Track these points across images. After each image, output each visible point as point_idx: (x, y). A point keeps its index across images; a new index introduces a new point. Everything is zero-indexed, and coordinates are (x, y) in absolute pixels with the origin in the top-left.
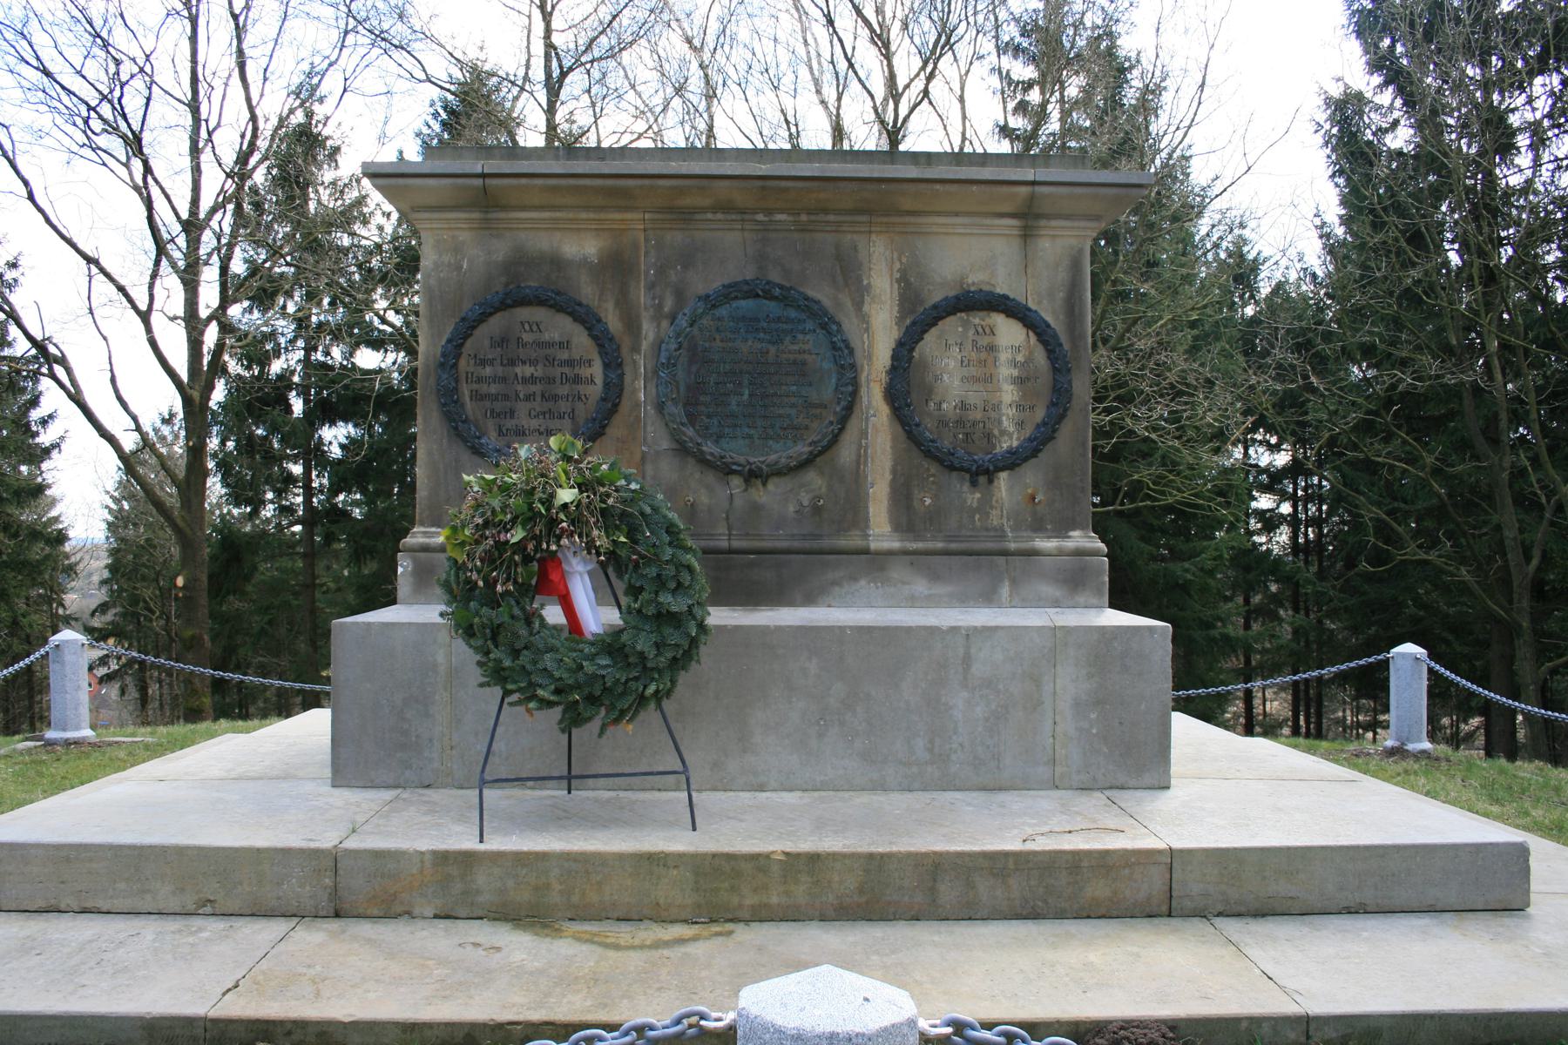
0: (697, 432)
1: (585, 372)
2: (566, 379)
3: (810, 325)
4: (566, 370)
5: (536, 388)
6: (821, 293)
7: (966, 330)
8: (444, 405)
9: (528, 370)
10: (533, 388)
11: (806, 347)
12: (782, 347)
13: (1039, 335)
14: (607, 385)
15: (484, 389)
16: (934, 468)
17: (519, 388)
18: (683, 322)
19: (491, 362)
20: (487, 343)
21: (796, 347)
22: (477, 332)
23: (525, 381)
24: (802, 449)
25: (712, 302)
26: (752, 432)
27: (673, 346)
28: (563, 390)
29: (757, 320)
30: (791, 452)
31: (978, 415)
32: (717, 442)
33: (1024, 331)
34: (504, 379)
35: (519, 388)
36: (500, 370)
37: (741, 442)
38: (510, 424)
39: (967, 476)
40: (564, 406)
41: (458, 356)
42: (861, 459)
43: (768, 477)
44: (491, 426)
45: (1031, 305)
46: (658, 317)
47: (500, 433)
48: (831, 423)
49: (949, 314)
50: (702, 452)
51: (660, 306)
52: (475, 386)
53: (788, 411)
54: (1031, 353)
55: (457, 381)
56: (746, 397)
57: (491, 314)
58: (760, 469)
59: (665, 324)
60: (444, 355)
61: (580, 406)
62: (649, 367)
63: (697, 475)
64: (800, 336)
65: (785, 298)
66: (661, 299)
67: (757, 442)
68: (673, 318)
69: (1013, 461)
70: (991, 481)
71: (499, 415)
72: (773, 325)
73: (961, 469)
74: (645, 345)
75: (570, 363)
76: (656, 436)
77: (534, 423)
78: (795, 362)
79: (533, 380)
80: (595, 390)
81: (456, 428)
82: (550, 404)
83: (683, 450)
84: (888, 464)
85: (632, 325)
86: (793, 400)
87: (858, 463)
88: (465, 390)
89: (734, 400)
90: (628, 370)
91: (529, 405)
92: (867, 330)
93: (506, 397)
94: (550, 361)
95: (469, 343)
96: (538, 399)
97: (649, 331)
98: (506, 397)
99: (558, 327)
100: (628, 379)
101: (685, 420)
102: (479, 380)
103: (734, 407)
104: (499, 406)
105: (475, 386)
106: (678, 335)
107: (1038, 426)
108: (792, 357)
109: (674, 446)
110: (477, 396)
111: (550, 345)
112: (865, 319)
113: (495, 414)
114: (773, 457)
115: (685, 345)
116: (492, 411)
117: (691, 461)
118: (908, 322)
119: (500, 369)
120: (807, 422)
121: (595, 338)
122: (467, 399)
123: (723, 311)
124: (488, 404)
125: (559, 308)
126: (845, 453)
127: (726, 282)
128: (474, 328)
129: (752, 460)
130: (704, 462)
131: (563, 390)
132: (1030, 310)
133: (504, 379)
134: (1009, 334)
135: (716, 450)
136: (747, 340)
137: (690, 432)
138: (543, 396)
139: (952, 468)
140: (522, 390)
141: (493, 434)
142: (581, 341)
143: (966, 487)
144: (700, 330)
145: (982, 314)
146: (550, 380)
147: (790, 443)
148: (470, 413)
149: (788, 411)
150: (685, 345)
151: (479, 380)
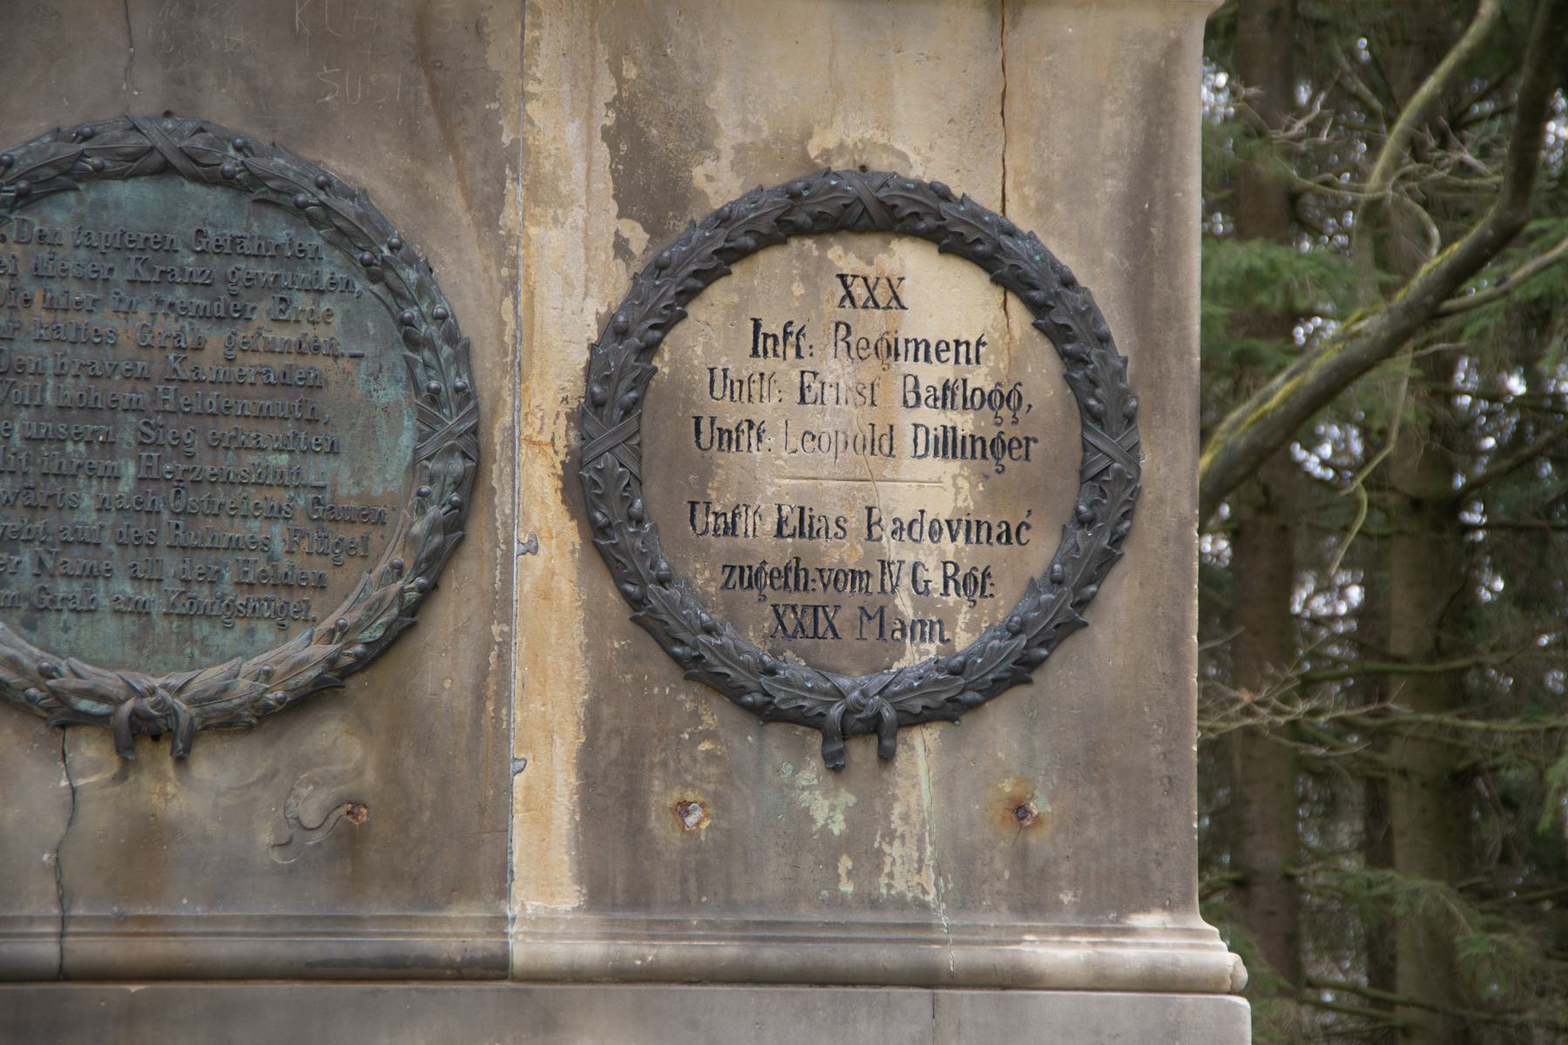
3: (331, 266)
11: (322, 333)
12: (244, 332)
24: (303, 651)
32: (30, 625)
43: (193, 736)
48: (399, 570)
56: (125, 487)
58: (172, 713)
64: (302, 301)
86: (280, 496)
103: (87, 515)
108: (277, 364)
114: (210, 676)
120: (320, 565)
127: (68, 122)
129: (144, 681)
147: (265, 631)
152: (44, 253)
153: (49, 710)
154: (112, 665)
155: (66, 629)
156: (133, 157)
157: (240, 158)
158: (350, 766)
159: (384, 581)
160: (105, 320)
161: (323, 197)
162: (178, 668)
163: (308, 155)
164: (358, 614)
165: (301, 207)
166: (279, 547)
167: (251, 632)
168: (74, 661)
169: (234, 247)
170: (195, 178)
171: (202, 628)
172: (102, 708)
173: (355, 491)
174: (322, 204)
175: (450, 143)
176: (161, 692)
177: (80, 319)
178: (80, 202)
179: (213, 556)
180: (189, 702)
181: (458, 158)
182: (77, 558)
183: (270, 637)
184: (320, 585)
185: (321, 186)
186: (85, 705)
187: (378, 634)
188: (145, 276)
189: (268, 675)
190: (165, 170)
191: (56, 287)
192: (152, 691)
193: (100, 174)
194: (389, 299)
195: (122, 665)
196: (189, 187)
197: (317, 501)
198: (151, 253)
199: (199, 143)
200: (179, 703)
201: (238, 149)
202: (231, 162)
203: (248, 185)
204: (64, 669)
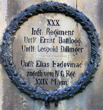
13: (83, 25)
31: (50, 69)
33: (75, 23)
39: (44, 103)
49: (35, 14)
54: (79, 35)
69: (68, 95)
70: (56, 106)
73: (39, 99)
107: (82, 75)
132: (78, 11)
134: (66, 24)
139: (34, 99)
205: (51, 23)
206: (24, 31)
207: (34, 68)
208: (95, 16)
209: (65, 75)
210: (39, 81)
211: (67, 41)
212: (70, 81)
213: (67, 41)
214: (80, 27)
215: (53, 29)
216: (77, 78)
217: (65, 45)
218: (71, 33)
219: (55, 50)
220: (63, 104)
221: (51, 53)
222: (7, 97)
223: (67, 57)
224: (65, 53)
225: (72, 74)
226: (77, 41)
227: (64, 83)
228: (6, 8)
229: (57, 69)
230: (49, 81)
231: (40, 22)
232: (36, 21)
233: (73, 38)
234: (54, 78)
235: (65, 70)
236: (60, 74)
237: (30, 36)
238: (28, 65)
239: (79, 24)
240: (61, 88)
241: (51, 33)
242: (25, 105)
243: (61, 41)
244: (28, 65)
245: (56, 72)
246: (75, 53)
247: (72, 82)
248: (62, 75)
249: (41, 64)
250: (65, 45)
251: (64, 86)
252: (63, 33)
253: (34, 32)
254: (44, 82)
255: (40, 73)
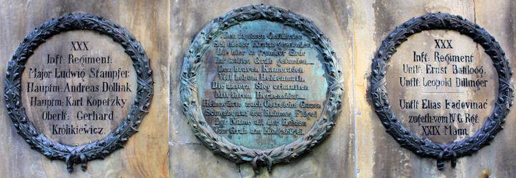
0: (214, 129)
1: (122, 81)
2: (107, 87)
3: (305, 40)
4: (107, 80)
5: (84, 95)
6: (313, 16)
7: (429, 45)
8: (9, 109)
9: (75, 81)
10: (80, 95)
11: (302, 58)
12: (282, 58)
13: (485, 47)
14: (139, 91)
15: (42, 96)
16: (407, 155)
17: (70, 95)
18: (201, 40)
19: (48, 74)
20: (45, 59)
21: (294, 59)
22: (37, 52)
23: (74, 89)
24: (301, 142)
25: (226, 24)
26: (260, 128)
27: (193, 59)
28: (104, 96)
29: (262, 37)
30: (290, 146)
31: (441, 112)
32: (230, 137)
33: (474, 44)
34: (57, 88)
35: (70, 95)
36: (54, 81)
37: (250, 137)
38: (62, 124)
39: (435, 162)
40: (105, 109)
41: (21, 71)
42: (349, 149)
43: (274, 165)
44: (46, 125)
45: (478, 23)
46: (181, 37)
47: (54, 131)
48: (325, 120)
49: (417, 31)
50: (217, 146)
51: (183, 27)
52: (34, 94)
53: (287, 110)
54: (480, 61)
55: (20, 90)
56: (254, 100)
57: (48, 37)
58: (266, 160)
59: (186, 41)
60: (9, 70)
61: (118, 109)
62: (174, 76)
63: (215, 165)
64: (297, 50)
65: (285, 19)
66: (184, 22)
67: (264, 137)
68: (193, 37)
69: (470, 150)
70: (453, 165)
71: (53, 117)
72: (275, 41)
73: (431, 156)
74: (171, 59)
75: (110, 74)
76: (181, 136)
77: (81, 124)
78: (293, 71)
79: (80, 88)
80: (130, 96)
81: (18, 128)
82: (94, 108)
83: (202, 144)
84: (372, 152)
85: (160, 43)
86: (293, 102)
87: (347, 153)
88: (27, 97)
89: (243, 102)
90: (157, 78)
91: (78, 108)
92: (351, 44)
93: (59, 102)
94: (94, 73)
95: (30, 60)
96: (85, 103)
97: (174, 48)
98: (59, 102)
99: (100, 46)
100: (157, 87)
101: (203, 120)
102: (38, 89)
103: (243, 109)
104: (53, 110)
105: (34, 94)
106: (198, 50)
108: (291, 66)
109: (195, 141)
110: (35, 102)
111: (94, 60)
112: (348, 36)
113: (50, 116)
114: (277, 150)
115: (203, 58)
116: (48, 114)
117: (209, 154)
118: (384, 37)
119: (55, 80)
120: (304, 119)
121: (130, 54)
122: (28, 104)
123: (234, 31)
124: (44, 108)
125: (100, 31)
126: (336, 145)
128: (34, 48)
129: (259, 152)
130: (219, 154)
131: (104, 96)
132: (478, 27)
133: (57, 88)
134: (462, 45)
135: (230, 145)
136: (253, 54)
137: (208, 129)
138: (88, 101)
139: (422, 156)
140: (72, 97)
141: (49, 132)
142: (119, 57)
143: (434, 169)
144: (216, 46)
145: (441, 32)
146: (94, 89)
147: (290, 137)
148: (30, 115)
149: (287, 110)
150: (203, 58)
151: (38, 89)
152: (231, 40)
153: (235, 160)
154: (251, 147)
155: (239, 138)
156: (253, 15)
157: (280, 14)
158: (314, 173)
159: (321, 124)
160: (246, 57)
161: (302, 22)
162: (268, 148)
163: (297, 13)
164: (316, 132)
165: (297, 25)
166: (293, 114)
167: (287, 138)
168: (242, 147)
169: (280, 36)
170: (268, 19)
171: (275, 137)
172: (249, 159)
173: (313, 99)
174: (302, 25)
175: (333, 8)
176: (264, 155)
177: (240, 57)
178: (240, 27)
179: (276, 118)
180: (272, 157)
181: (336, 13)
182: (241, 119)
183: (292, 139)
184: (304, 124)
185: (302, 20)
186: (245, 158)
187: (321, 137)
188: (257, 45)
189: (292, 149)
190: (262, 18)
191: (234, 49)
192: (262, 155)
193: (245, 20)
194: (320, 49)
195: (254, 148)
196: (267, 22)
197: (303, 102)
198: (258, 41)
199: (270, 10)
200: (269, 158)
201: (280, 11)
202: (278, 15)
203: (284, 20)
204: (239, 149)
205: (440, 44)
206: (402, 56)
207: (420, 111)
208: (502, 33)
209: (464, 119)
210: (427, 130)
211: (464, 70)
212: (471, 128)
213: (464, 70)
214: (481, 50)
215: (444, 52)
216: (481, 124)
217: (461, 76)
218: (469, 58)
219: (447, 83)
220: (462, 163)
221: (443, 88)
222: (380, 156)
223: (465, 94)
224: (462, 89)
225: (473, 119)
226: (478, 71)
227: (462, 131)
228: (373, 22)
229: (452, 111)
230: (441, 130)
231: (425, 44)
232: (419, 42)
233: (472, 66)
234: (449, 124)
235: (464, 112)
236: (456, 119)
237: (412, 64)
238: (410, 107)
239: (480, 46)
240: (459, 139)
241: (441, 59)
242: (408, 167)
243: (456, 71)
244: (410, 107)
245: (451, 115)
246: (476, 88)
247: (473, 130)
248: (460, 121)
249: (430, 105)
250: (461, 76)
251: (464, 137)
252: (459, 59)
253: (416, 57)
254: (433, 131)
255: (428, 118)
